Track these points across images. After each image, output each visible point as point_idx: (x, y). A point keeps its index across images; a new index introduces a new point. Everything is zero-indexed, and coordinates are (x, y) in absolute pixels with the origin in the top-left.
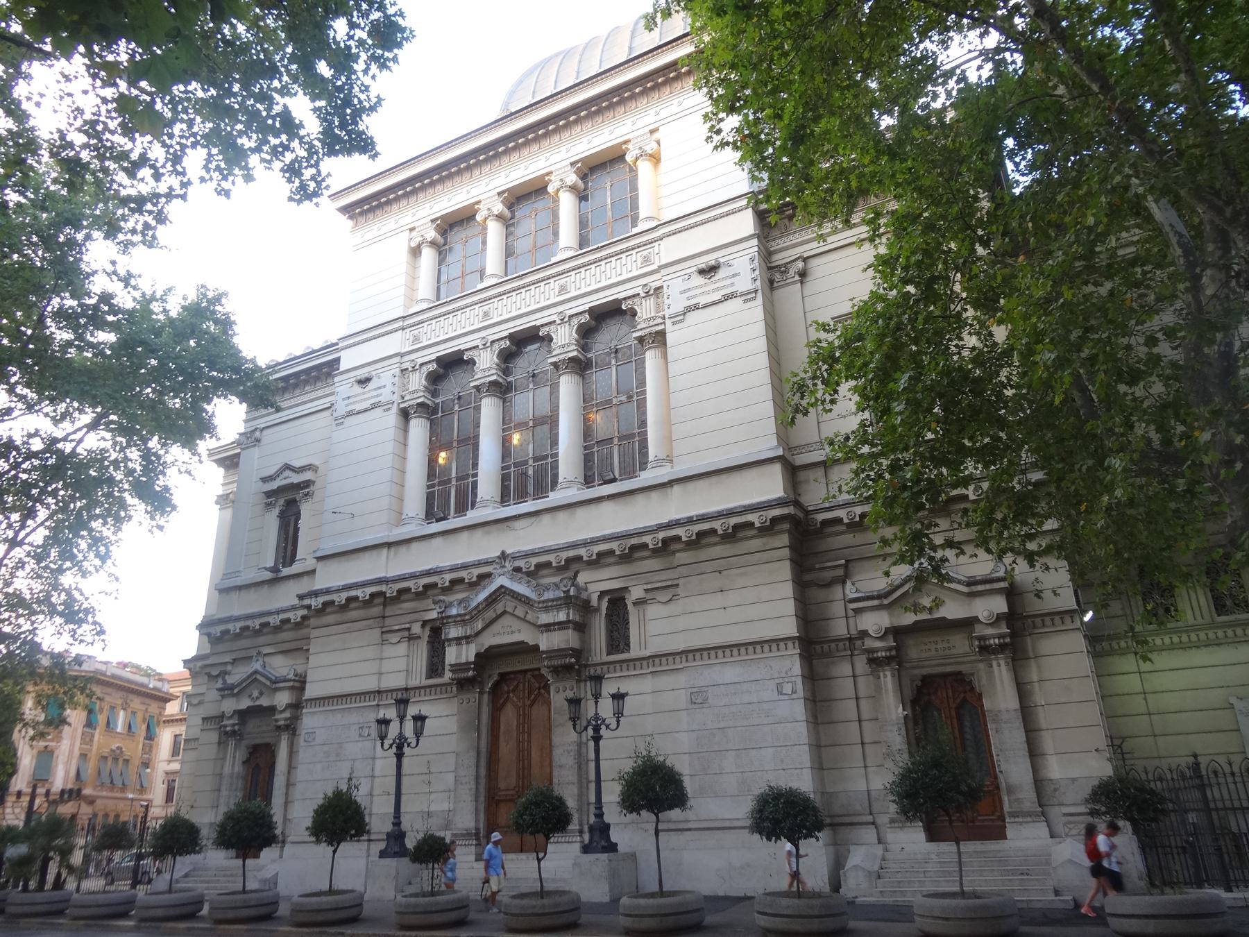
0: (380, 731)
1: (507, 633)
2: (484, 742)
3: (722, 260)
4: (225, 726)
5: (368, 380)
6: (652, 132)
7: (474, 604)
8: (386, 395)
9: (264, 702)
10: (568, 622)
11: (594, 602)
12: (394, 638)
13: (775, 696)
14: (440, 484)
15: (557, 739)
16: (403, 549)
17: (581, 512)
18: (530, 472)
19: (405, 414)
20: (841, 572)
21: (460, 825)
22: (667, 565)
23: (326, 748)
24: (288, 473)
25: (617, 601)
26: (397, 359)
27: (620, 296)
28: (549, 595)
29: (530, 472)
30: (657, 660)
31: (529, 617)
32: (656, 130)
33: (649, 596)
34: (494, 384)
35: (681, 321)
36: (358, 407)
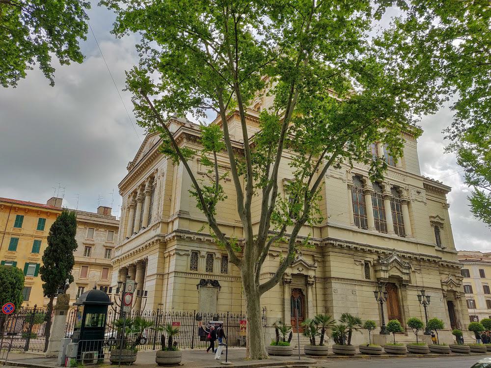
9: (304, 273)
16: (355, 234)
31: (401, 269)
36: (335, 176)
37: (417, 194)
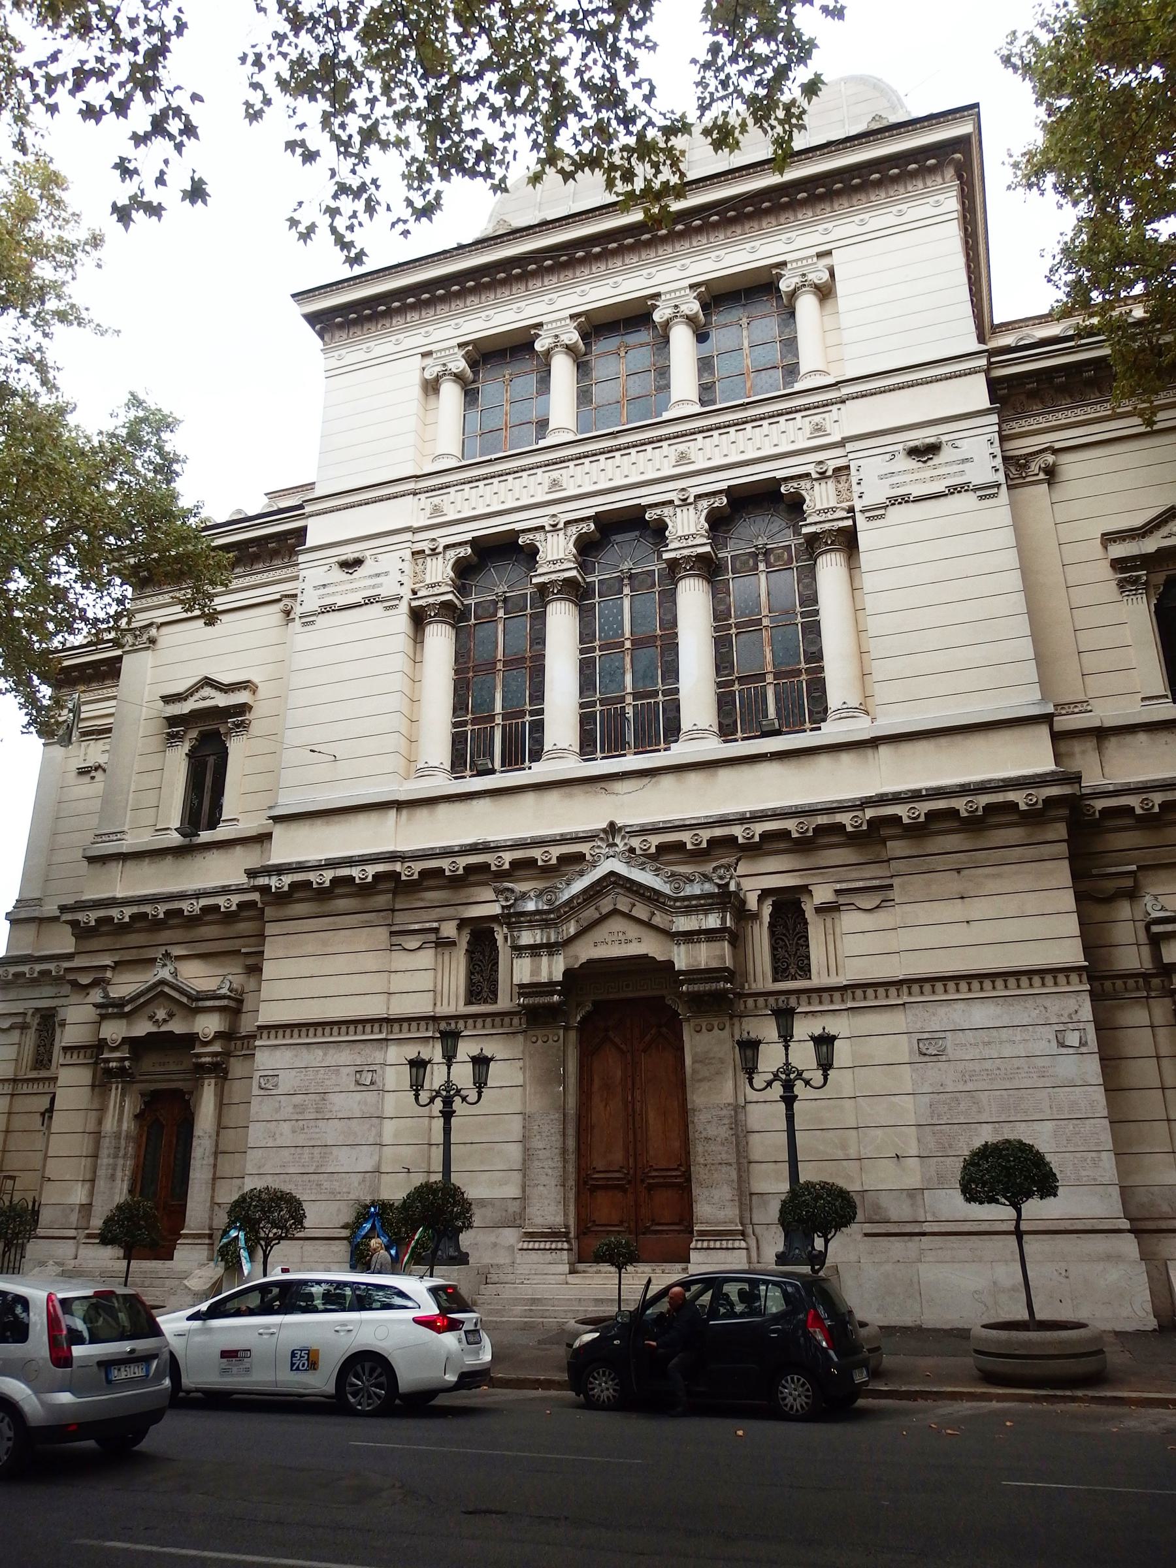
0: (744, 1059)
1: (619, 942)
2: (572, 1102)
3: (944, 438)
4: (108, 1060)
5: (358, 562)
6: (820, 255)
7: (565, 896)
8: (388, 588)
9: (177, 1027)
10: (723, 930)
11: (752, 903)
12: (412, 943)
13: (1054, 1048)
14: (474, 721)
15: (698, 1098)
16: (422, 813)
17: (724, 774)
18: (630, 712)
19: (419, 618)
20: (1129, 883)
21: (539, 1220)
22: (872, 857)
23: (298, 1099)
24: (207, 691)
25: (788, 908)
26: (408, 536)
27: (779, 474)
28: (696, 889)
29: (630, 712)
30: (859, 992)
31: (658, 920)
32: (829, 253)
33: (842, 900)
34: (700, 557)
35: (882, 516)
36: (341, 601)
37: (912, 464)
